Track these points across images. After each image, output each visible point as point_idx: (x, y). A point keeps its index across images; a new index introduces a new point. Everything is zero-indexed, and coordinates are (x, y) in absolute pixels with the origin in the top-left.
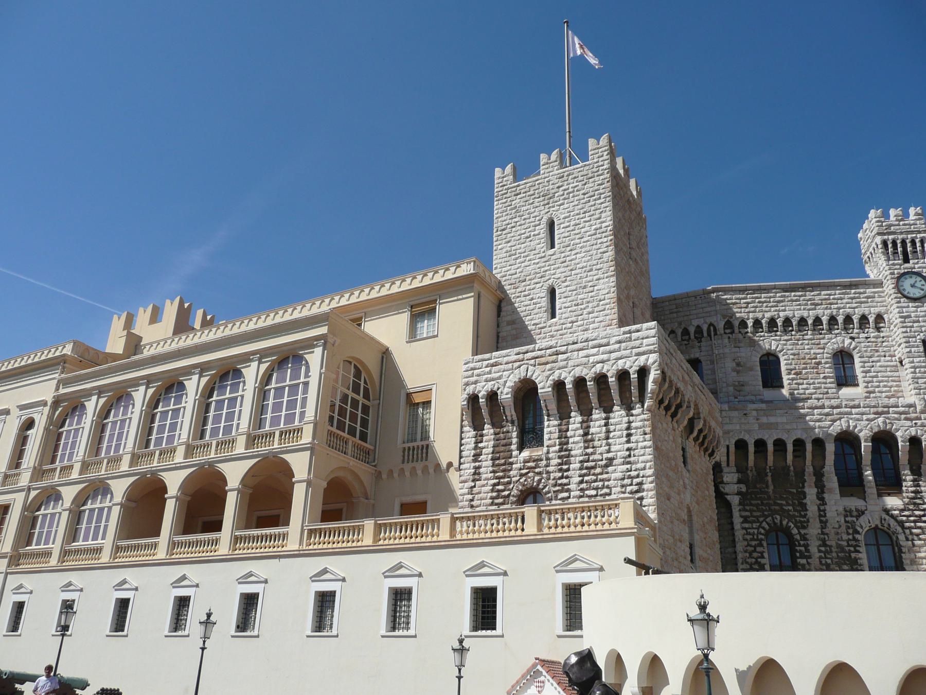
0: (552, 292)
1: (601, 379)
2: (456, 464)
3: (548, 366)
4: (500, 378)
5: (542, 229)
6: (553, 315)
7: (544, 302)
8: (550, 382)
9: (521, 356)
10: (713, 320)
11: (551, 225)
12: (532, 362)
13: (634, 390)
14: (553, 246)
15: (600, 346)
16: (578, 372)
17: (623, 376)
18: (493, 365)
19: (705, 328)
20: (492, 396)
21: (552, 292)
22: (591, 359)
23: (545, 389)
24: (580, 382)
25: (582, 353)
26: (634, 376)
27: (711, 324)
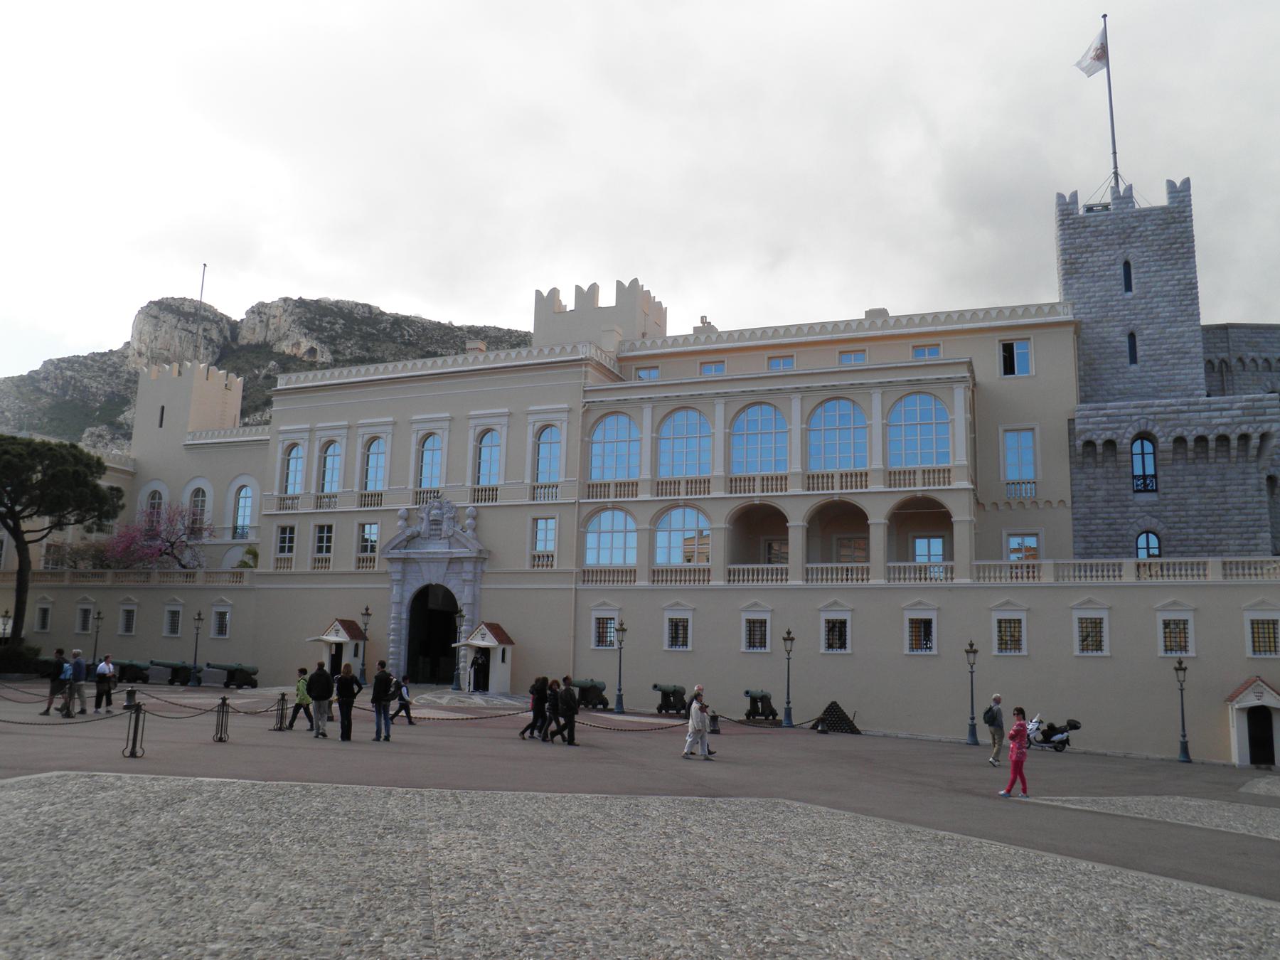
0: (1132, 337)
1: (1223, 439)
2: (1069, 503)
3: (1171, 423)
4: (1118, 428)
5: (1119, 270)
6: (1133, 359)
7: (1125, 347)
8: (1170, 439)
9: (1139, 410)
10: (1224, 355)
11: (1127, 265)
12: (1151, 417)
13: (1253, 452)
14: (1128, 287)
15: (1222, 410)
16: (1201, 431)
17: (1244, 438)
18: (1108, 416)
19: (1216, 362)
20: (1110, 444)
21: (1132, 337)
22: (1214, 421)
23: (1165, 443)
24: (1201, 440)
25: (1203, 415)
26: (1255, 442)
27: (1223, 361)
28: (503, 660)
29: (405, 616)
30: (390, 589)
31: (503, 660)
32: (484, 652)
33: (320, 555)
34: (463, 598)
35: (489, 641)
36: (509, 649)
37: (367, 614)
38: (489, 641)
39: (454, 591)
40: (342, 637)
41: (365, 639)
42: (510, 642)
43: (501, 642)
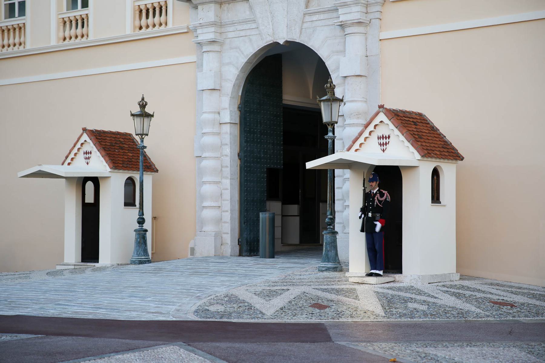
28: (436, 198)
29: (226, 117)
30: (199, 65)
31: (436, 198)
32: (387, 180)
33: (72, 14)
34: (342, 63)
35: (400, 151)
36: (449, 172)
37: (143, 114)
38: (400, 151)
39: (322, 53)
40: (98, 165)
41: (149, 167)
42: (450, 153)
43: (427, 152)
